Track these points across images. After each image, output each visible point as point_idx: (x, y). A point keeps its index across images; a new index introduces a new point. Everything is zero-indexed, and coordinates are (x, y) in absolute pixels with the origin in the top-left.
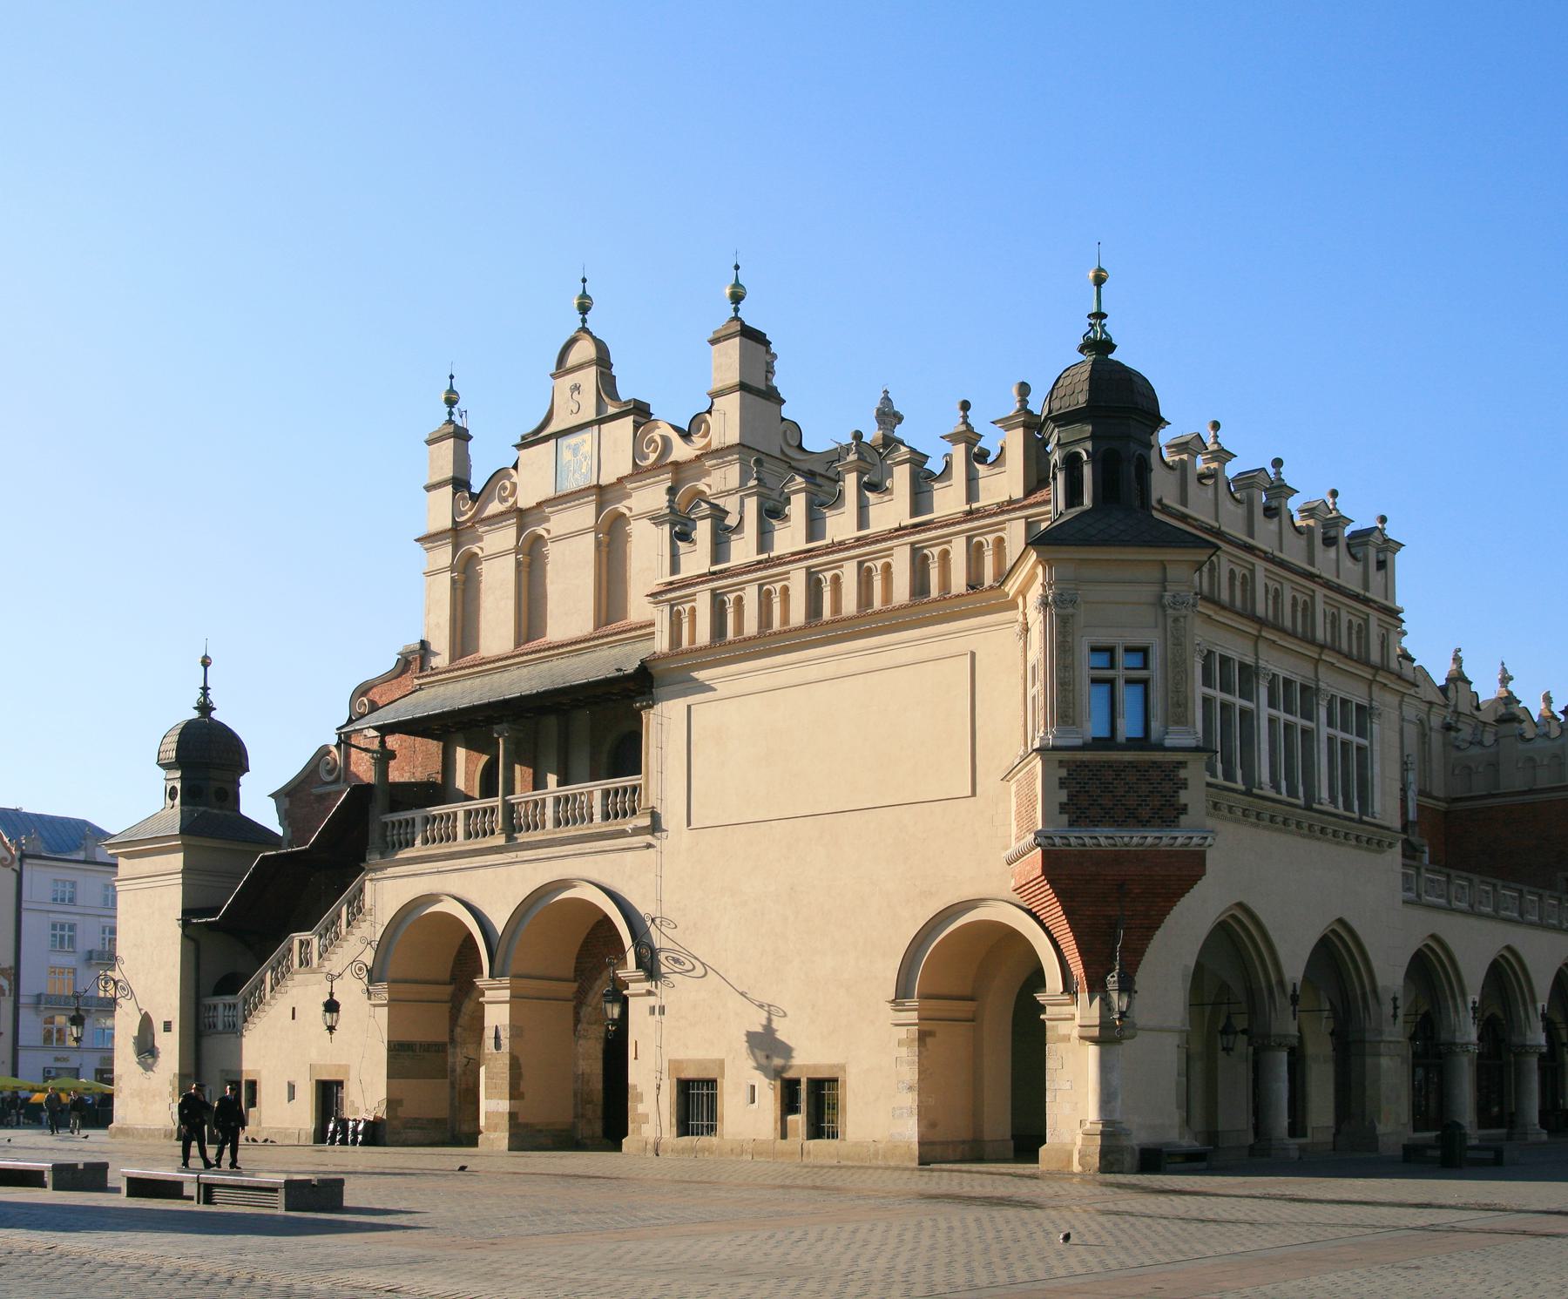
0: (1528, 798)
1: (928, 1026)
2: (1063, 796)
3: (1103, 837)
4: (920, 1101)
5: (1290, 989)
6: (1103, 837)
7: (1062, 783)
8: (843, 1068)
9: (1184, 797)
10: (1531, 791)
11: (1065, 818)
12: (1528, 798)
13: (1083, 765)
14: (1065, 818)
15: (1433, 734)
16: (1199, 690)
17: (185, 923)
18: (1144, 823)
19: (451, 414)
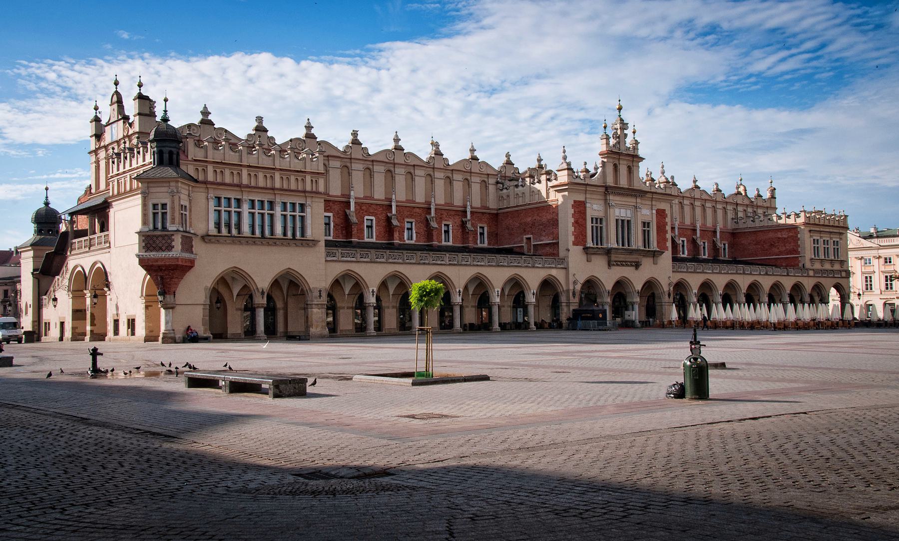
0: (516, 209)
1: (149, 304)
2: (144, 244)
3: (153, 254)
4: (146, 325)
5: (261, 291)
6: (153, 254)
7: (143, 241)
8: (135, 316)
9: (173, 244)
10: (517, 206)
11: (144, 250)
12: (516, 209)
13: (149, 236)
14: (144, 250)
15: (490, 186)
16: (187, 213)
17: (32, 274)
18: (163, 251)
19: (96, 113)
